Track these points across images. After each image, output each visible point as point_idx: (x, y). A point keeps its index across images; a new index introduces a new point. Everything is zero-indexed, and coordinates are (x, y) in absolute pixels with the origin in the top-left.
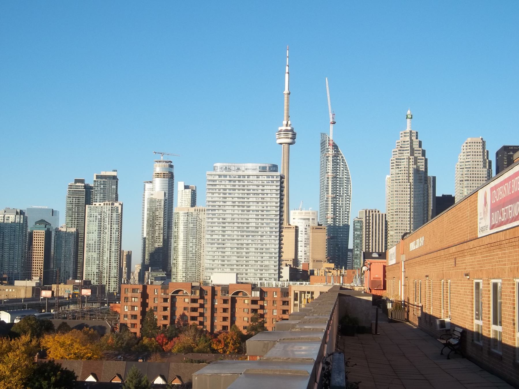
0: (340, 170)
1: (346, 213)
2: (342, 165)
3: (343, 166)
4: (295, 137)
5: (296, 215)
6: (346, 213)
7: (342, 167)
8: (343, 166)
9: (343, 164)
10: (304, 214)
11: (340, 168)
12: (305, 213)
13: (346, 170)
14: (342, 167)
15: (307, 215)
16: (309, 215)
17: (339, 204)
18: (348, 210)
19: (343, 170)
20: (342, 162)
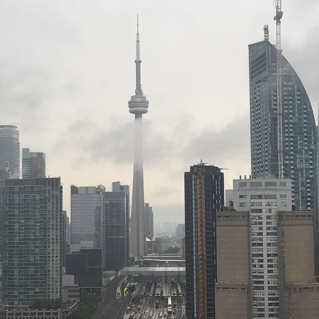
0: (294, 106)
1: (308, 181)
2: (298, 95)
3: (299, 98)
4: (148, 105)
5: (245, 188)
6: (308, 181)
7: (298, 100)
8: (299, 98)
9: (299, 93)
10: (263, 187)
11: (294, 101)
12: (267, 184)
13: (305, 104)
14: (298, 100)
15: (271, 187)
16: (274, 187)
17: (295, 165)
18: (311, 176)
19: (298, 104)
20: (298, 91)
